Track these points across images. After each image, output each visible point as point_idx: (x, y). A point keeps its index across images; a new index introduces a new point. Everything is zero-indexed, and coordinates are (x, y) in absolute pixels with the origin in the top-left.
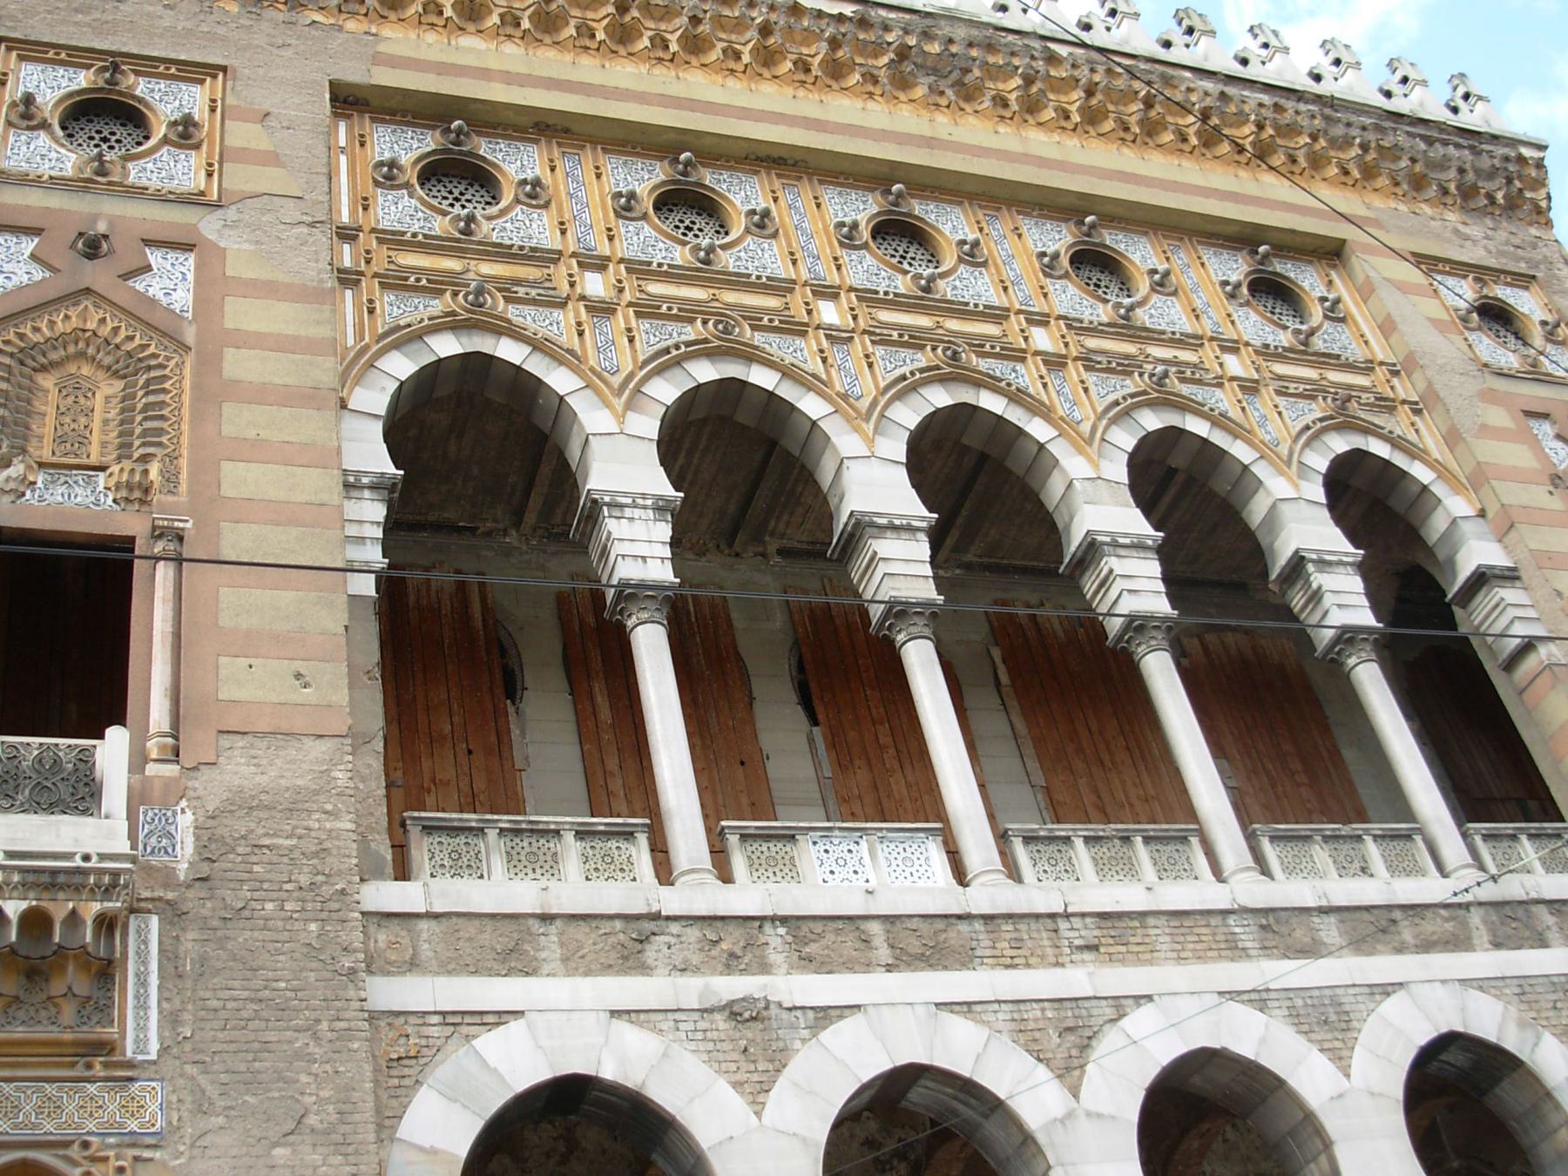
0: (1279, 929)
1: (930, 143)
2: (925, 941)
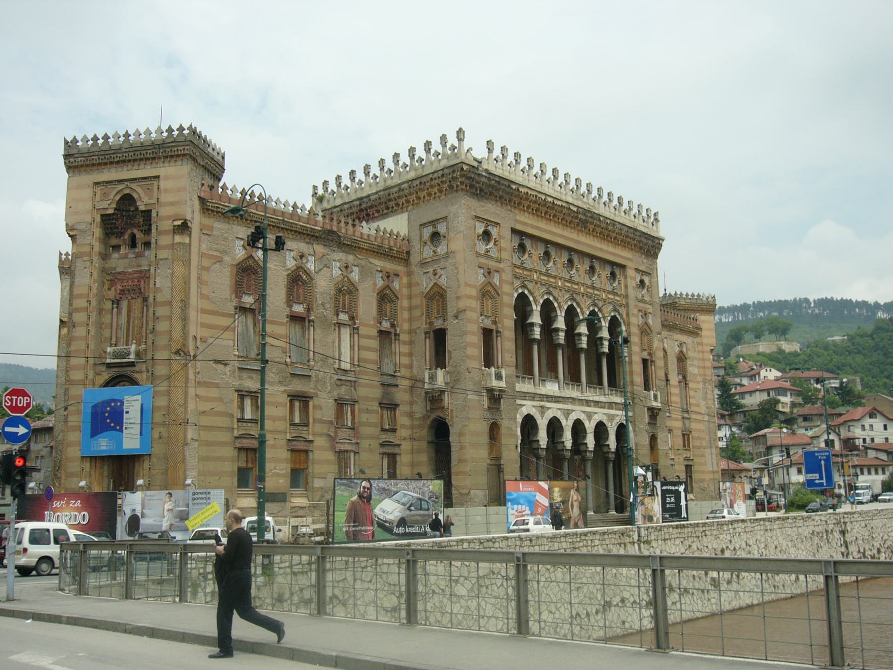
0: (588, 402)
1: (578, 242)
2: (557, 399)
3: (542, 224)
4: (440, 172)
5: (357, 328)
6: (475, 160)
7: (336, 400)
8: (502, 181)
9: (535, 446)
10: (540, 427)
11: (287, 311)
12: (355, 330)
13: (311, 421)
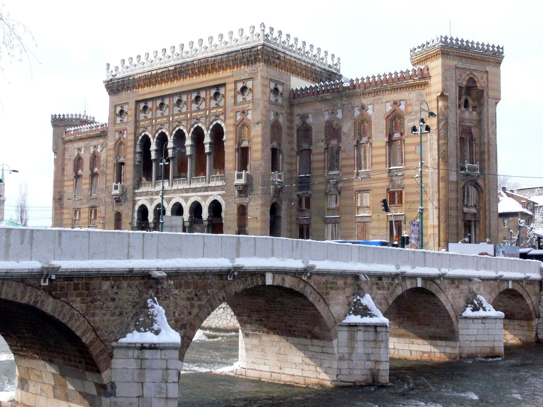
0: (187, 191)
3: (157, 87)
10: (149, 211)
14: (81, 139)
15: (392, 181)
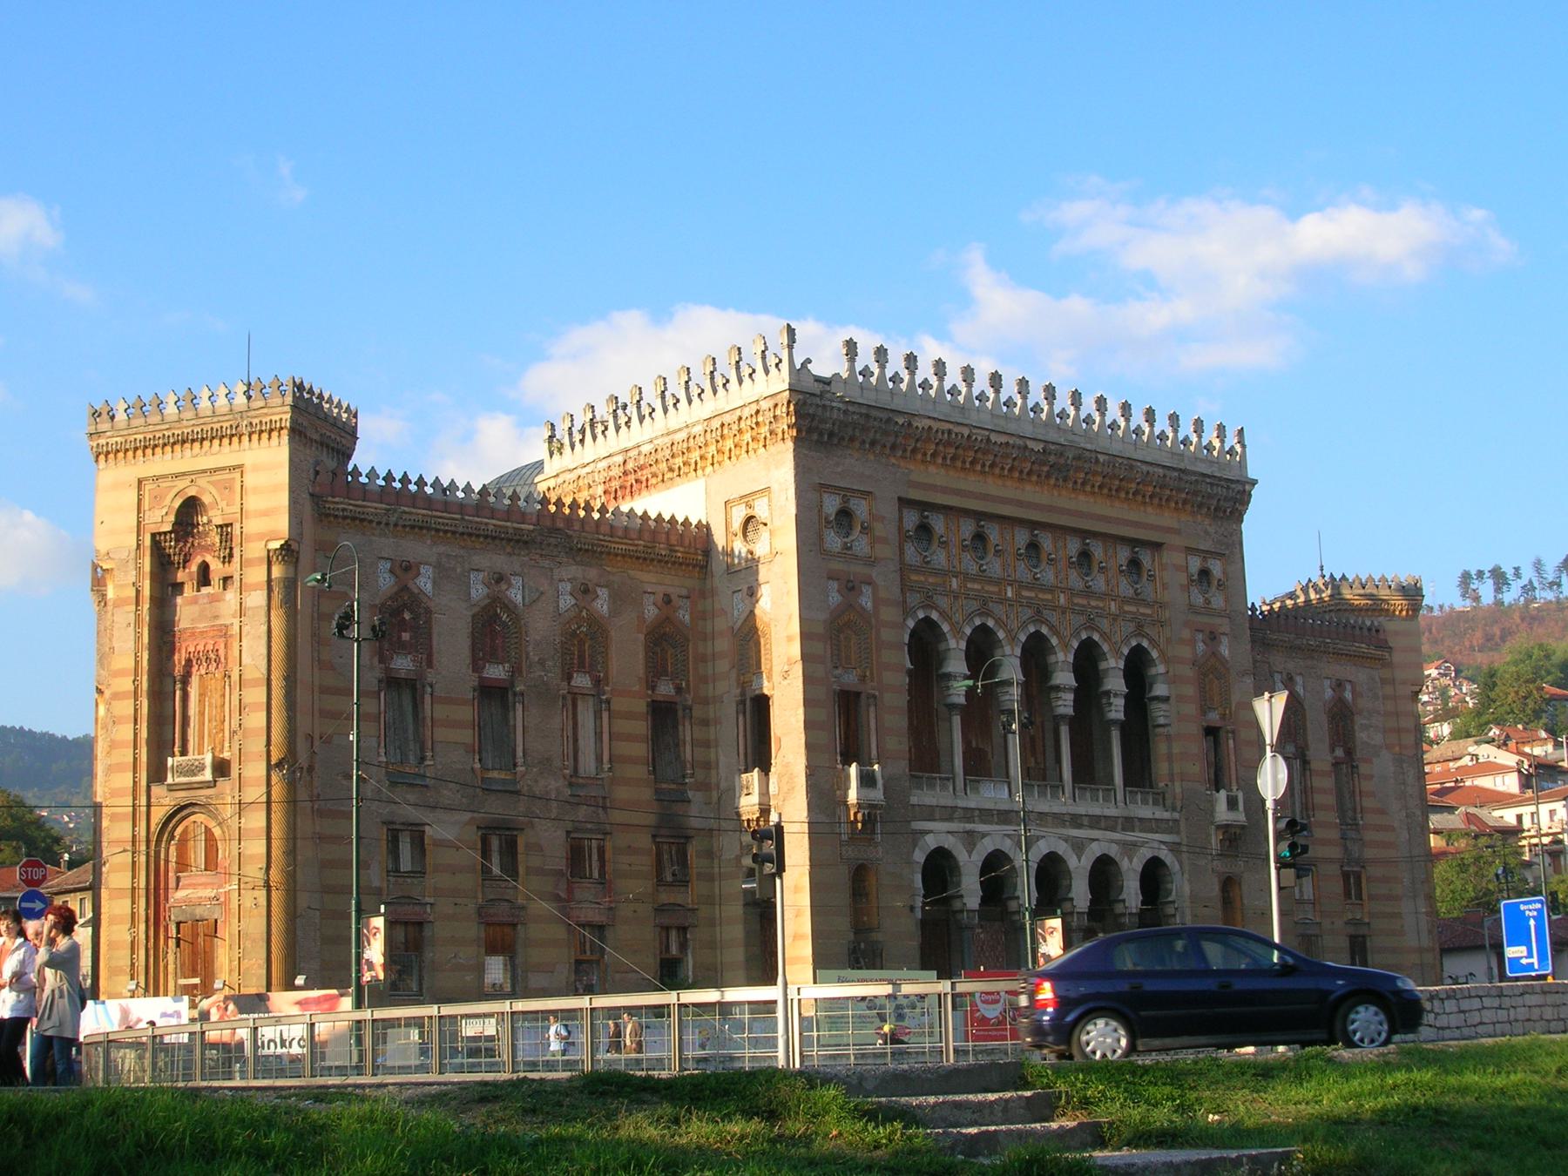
0: (1076, 821)
2: (1005, 817)
3: (972, 483)
4: (754, 407)
5: (608, 702)
6: (818, 380)
7: (568, 833)
8: (874, 413)
9: (957, 905)
11: (472, 680)
12: (602, 705)
13: (521, 870)
14: (418, 528)
15: (1346, 849)
